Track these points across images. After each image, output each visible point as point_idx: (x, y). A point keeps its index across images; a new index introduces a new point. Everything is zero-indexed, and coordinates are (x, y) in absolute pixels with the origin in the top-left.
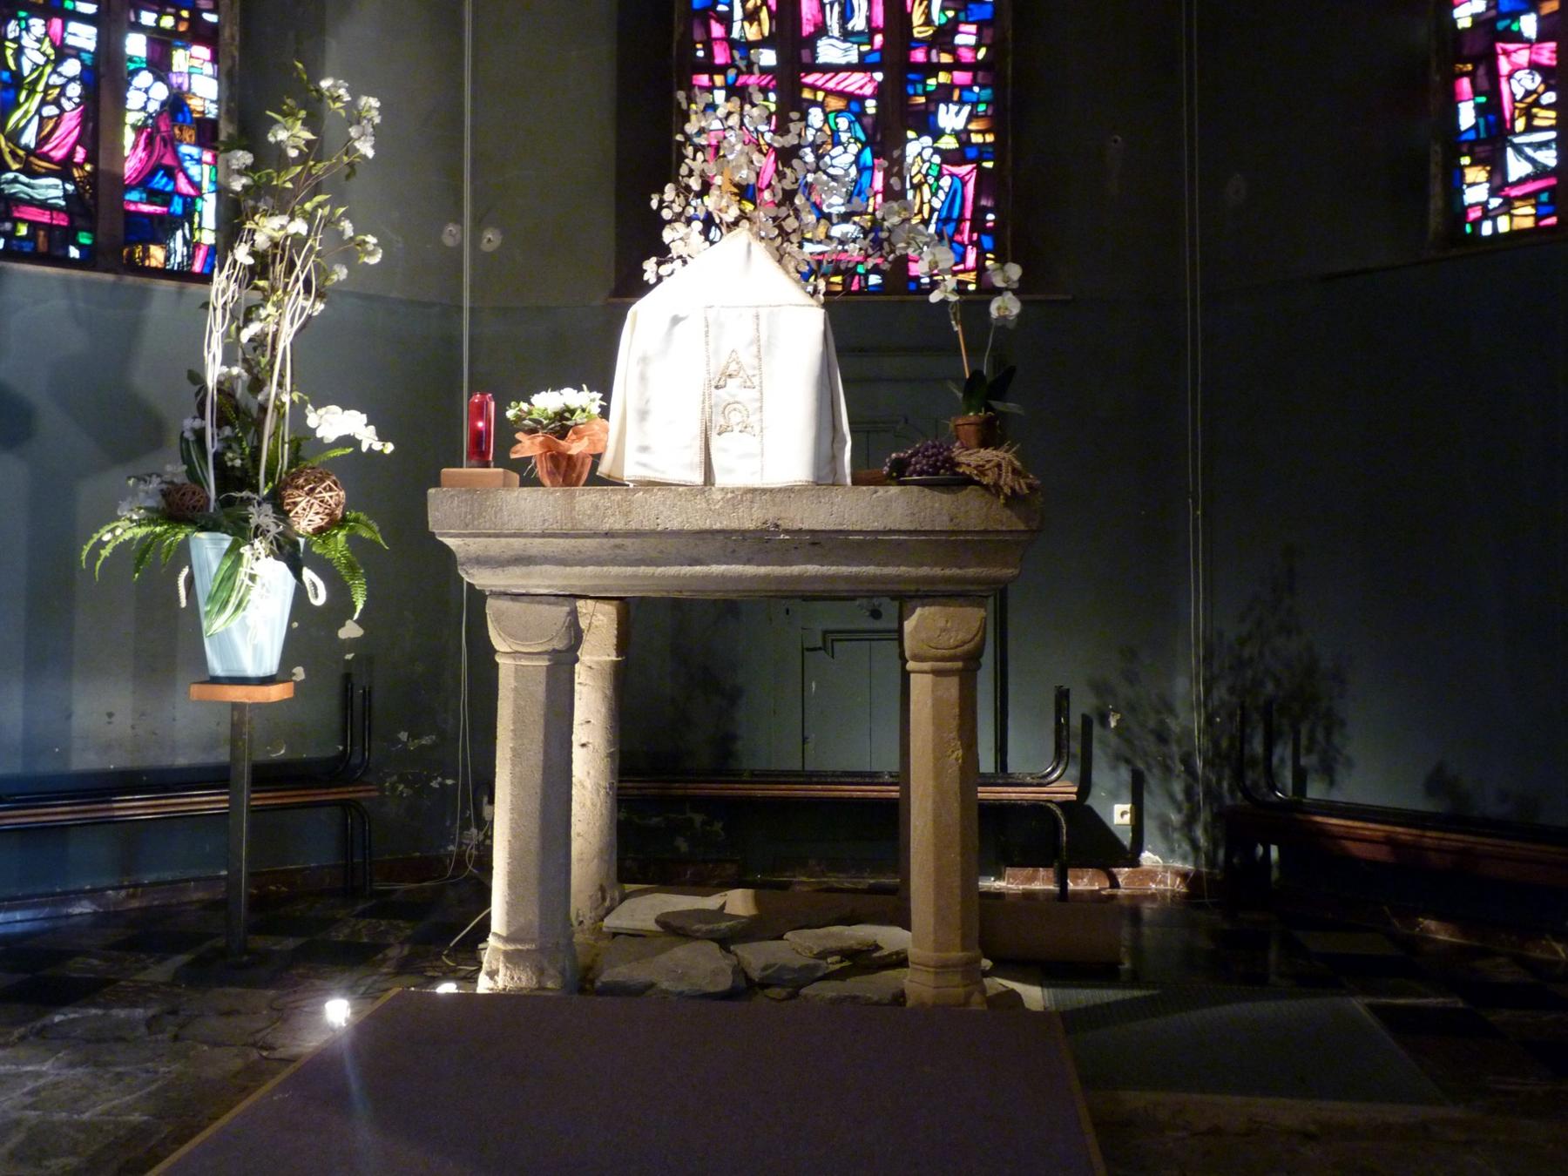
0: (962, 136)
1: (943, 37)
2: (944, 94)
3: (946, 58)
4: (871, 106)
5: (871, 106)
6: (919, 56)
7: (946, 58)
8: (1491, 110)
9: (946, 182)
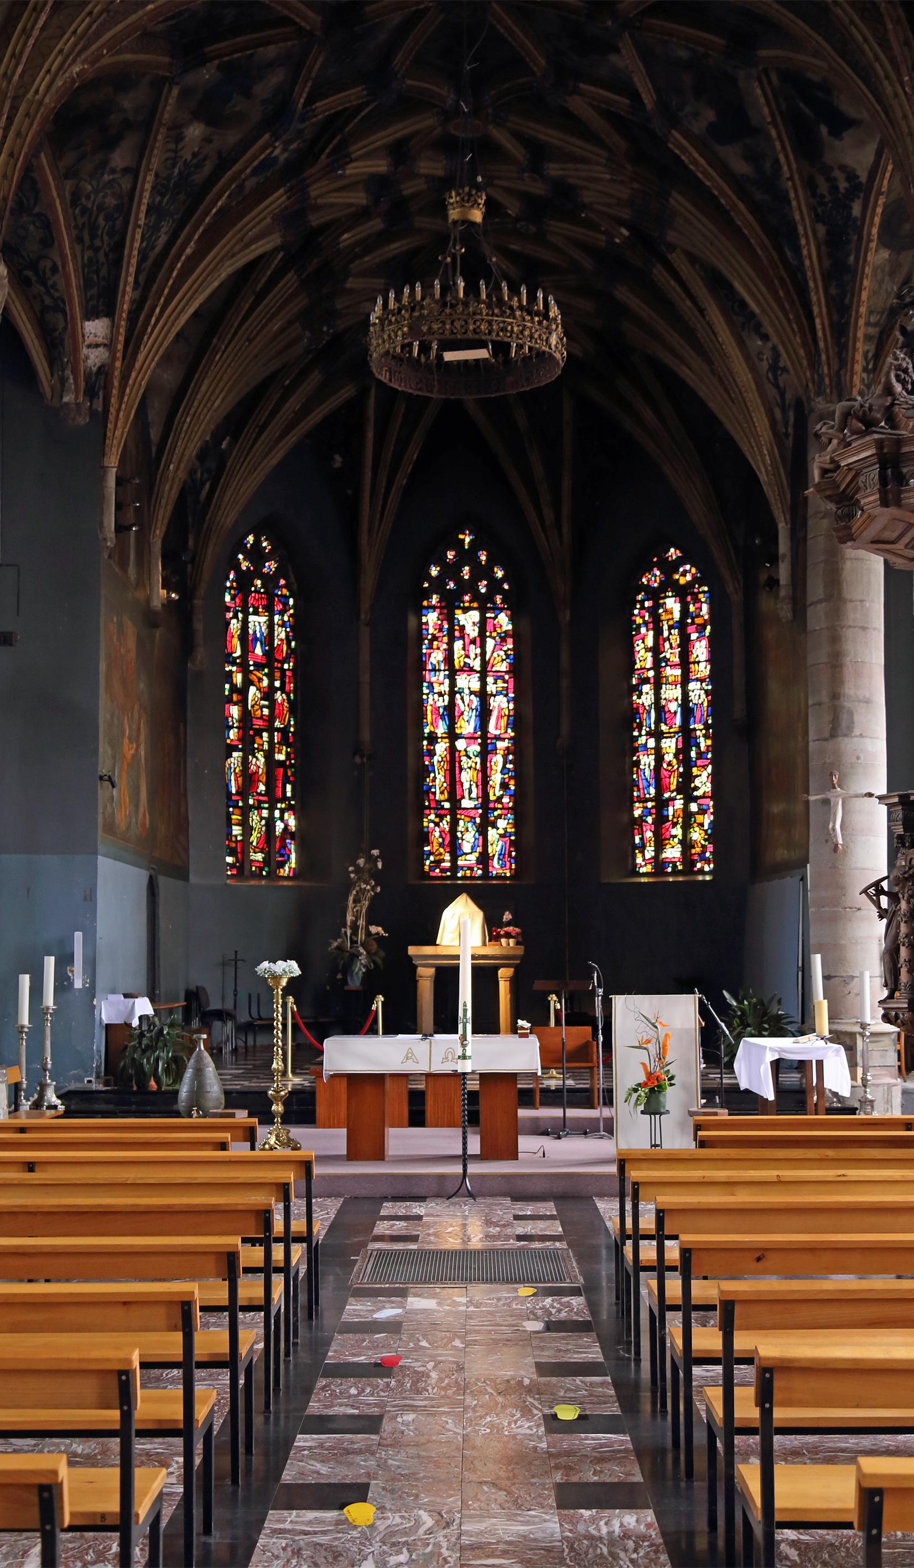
0: (505, 829)
1: (499, 800)
2: (500, 816)
3: (500, 806)
4: (478, 820)
6: (491, 805)
7: (500, 806)
8: (642, 839)
9: (500, 843)
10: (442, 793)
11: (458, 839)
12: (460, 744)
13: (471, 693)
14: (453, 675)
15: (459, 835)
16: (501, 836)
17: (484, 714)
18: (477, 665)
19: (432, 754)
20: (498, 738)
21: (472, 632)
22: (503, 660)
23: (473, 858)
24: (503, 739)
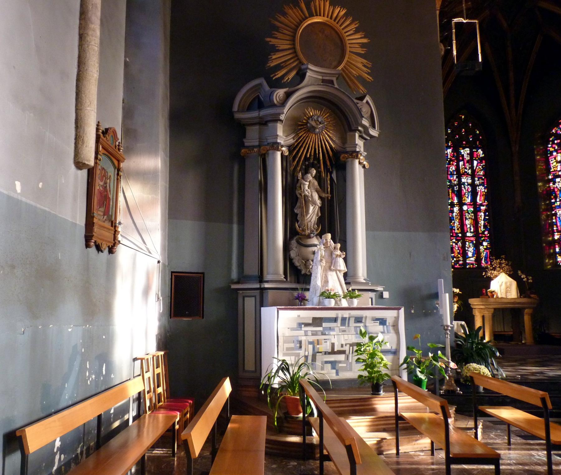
0: (487, 246)
1: (483, 232)
2: (484, 240)
4: (474, 242)
5: (474, 242)
6: (480, 235)
10: (458, 229)
11: (466, 250)
12: (465, 208)
13: (468, 185)
14: (459, 176)
15: (467, 249)
16: (485, 249)
17: (474, 194)
18: (470, 171)
19: (452, 212)
20: (481, 205)
21: (467, 158)
22: (481, 170)
23: (473, 259)
24: (483, 206)
